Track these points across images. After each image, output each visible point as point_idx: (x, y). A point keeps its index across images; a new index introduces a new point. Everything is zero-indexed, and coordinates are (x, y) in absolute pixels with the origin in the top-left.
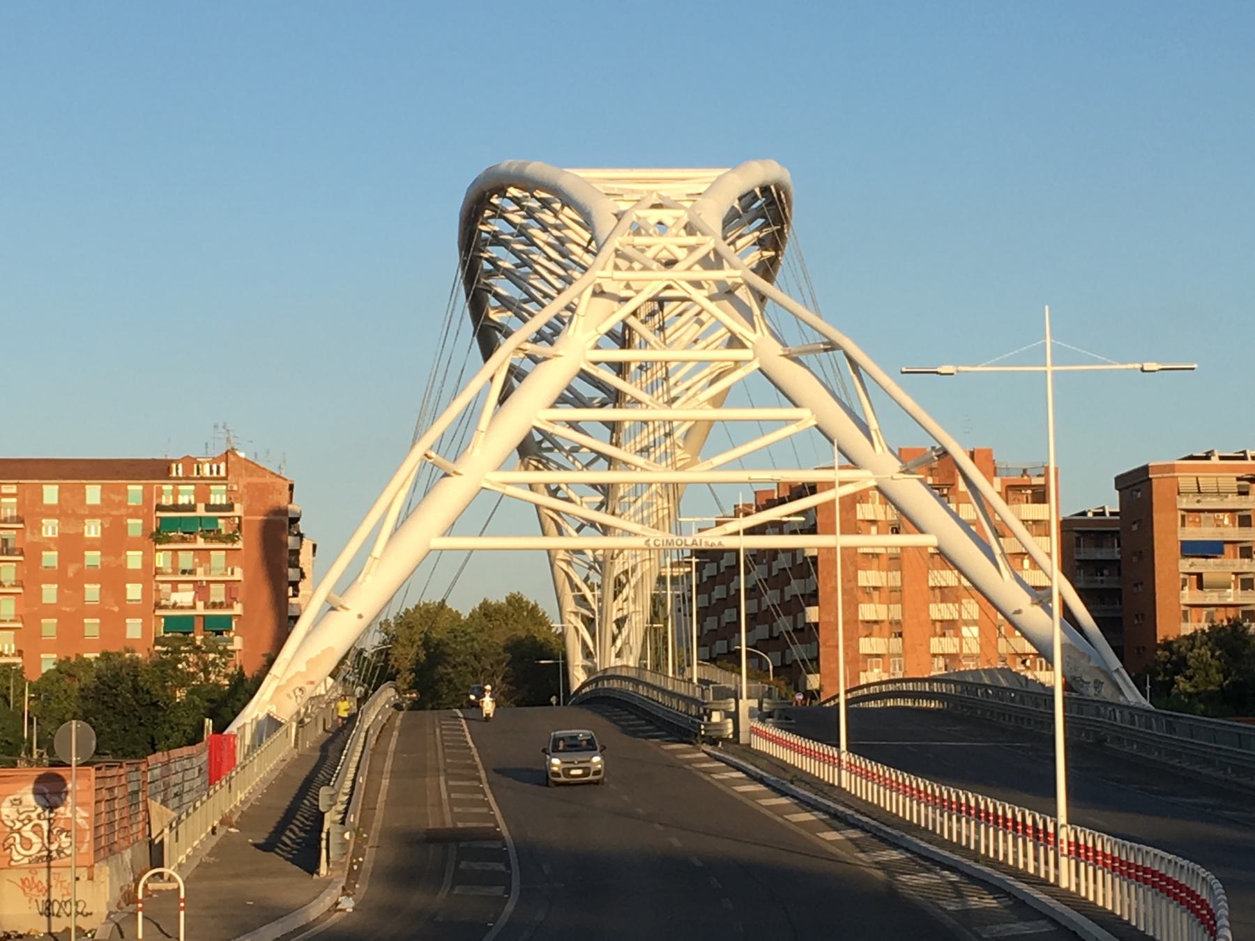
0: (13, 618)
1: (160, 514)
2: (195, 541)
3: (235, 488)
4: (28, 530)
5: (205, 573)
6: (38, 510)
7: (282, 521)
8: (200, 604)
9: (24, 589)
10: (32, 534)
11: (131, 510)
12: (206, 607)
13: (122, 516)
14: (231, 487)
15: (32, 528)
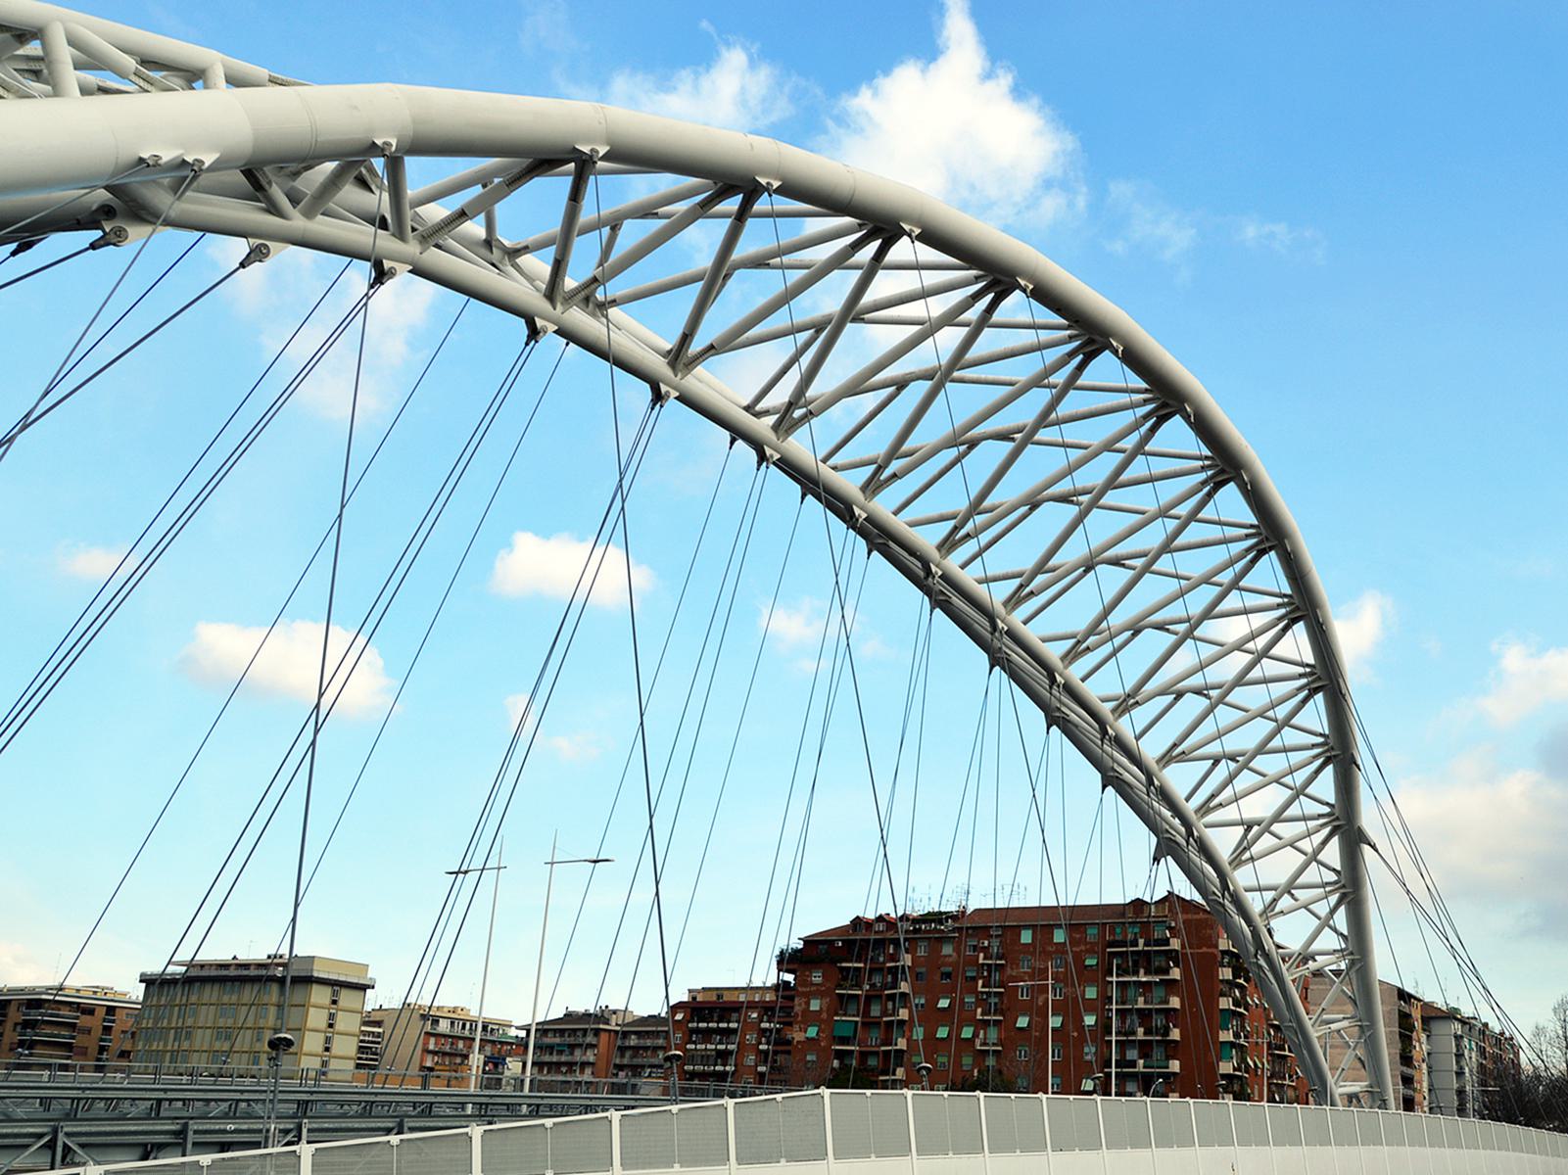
0: (995, 1041)
1: (1108, 950)
2: (1136, 973)
3: (1173, 924)
4: (1009, 965)
5: (1146, 1002)
6: (1016, 948)
7: (1213, 953)
8: (1141, 1030)
9: (1004, 1017)
10: (1012, 969)
11: (1088, 947)
12: (1145, 1034)
13: (1081, 951)
14: (1170, 924)
15: (1011, 964)
